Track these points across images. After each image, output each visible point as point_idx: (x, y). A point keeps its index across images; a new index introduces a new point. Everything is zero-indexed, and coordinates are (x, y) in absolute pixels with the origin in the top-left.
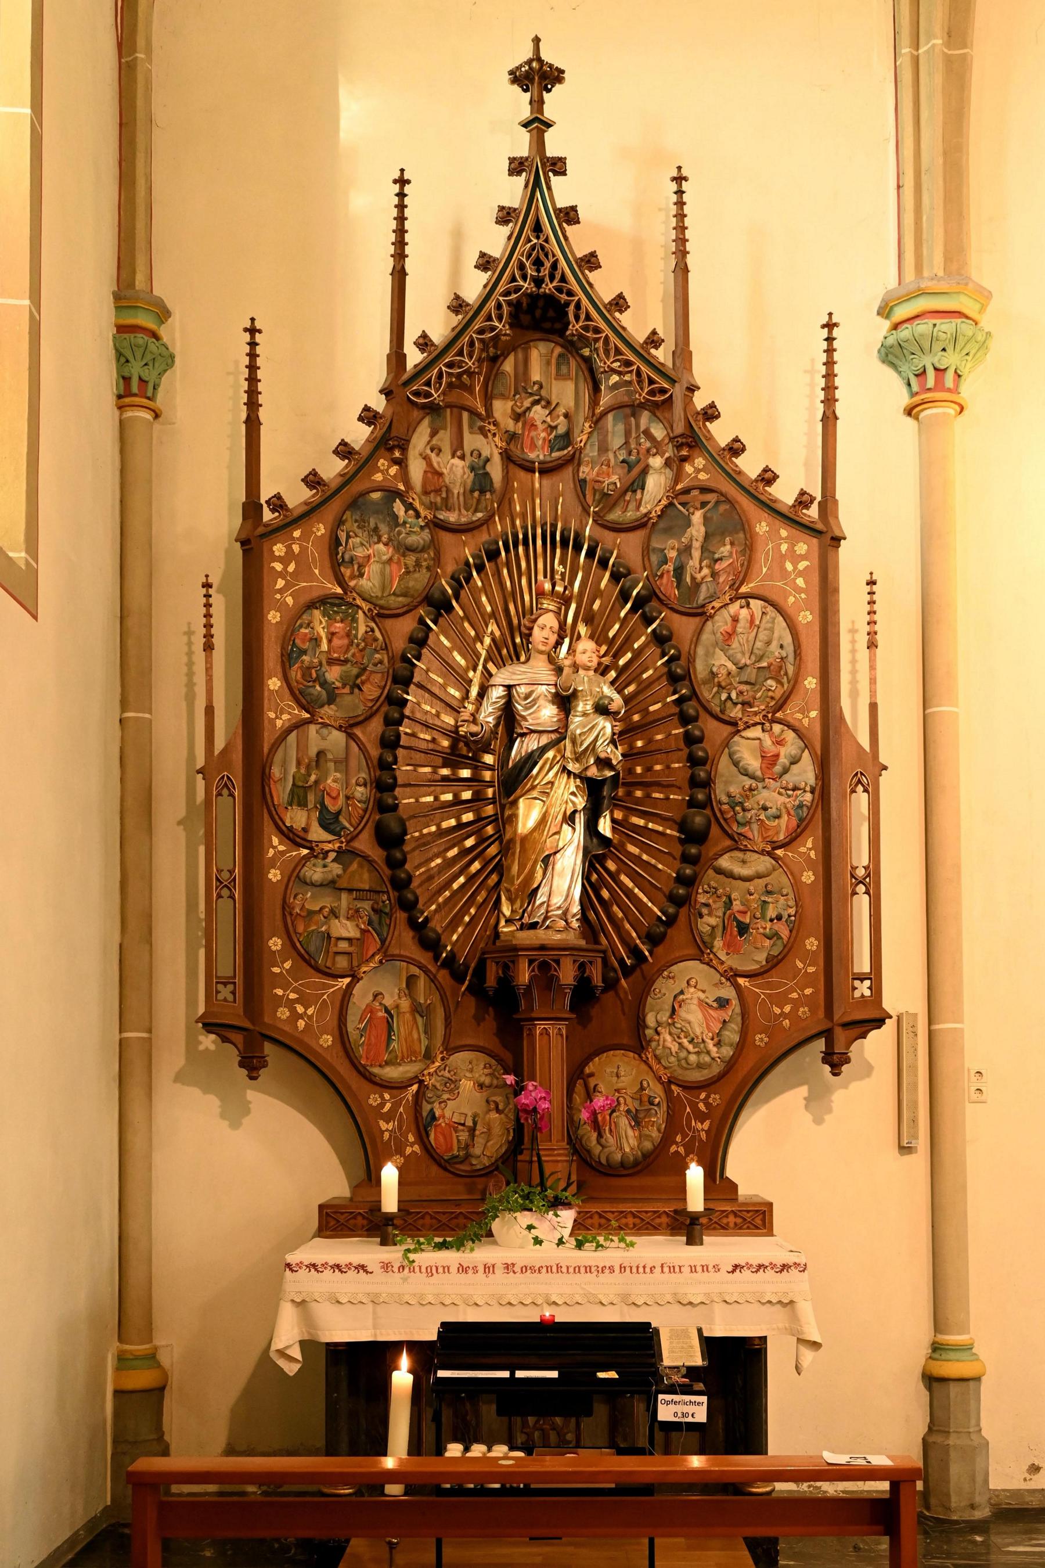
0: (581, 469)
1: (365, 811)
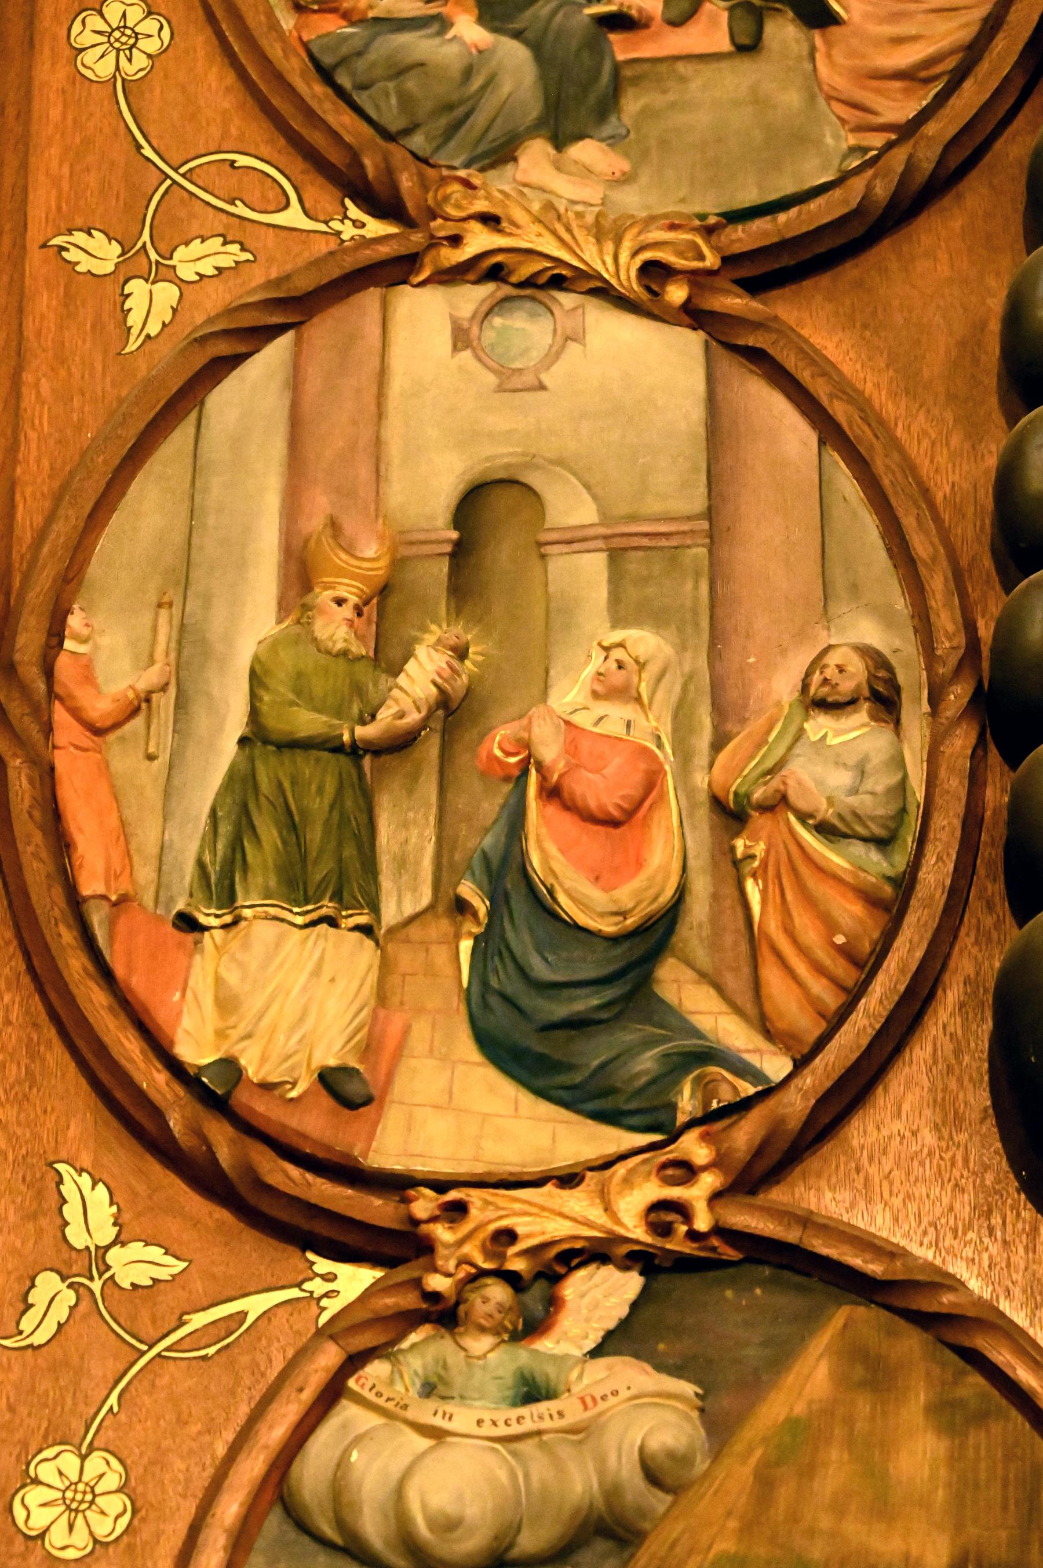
1: (892, 904)
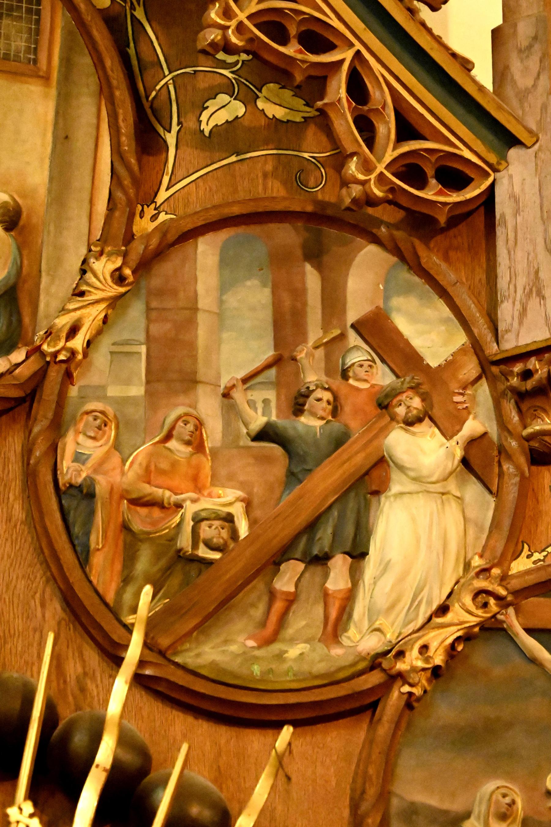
0: (72, 443)
